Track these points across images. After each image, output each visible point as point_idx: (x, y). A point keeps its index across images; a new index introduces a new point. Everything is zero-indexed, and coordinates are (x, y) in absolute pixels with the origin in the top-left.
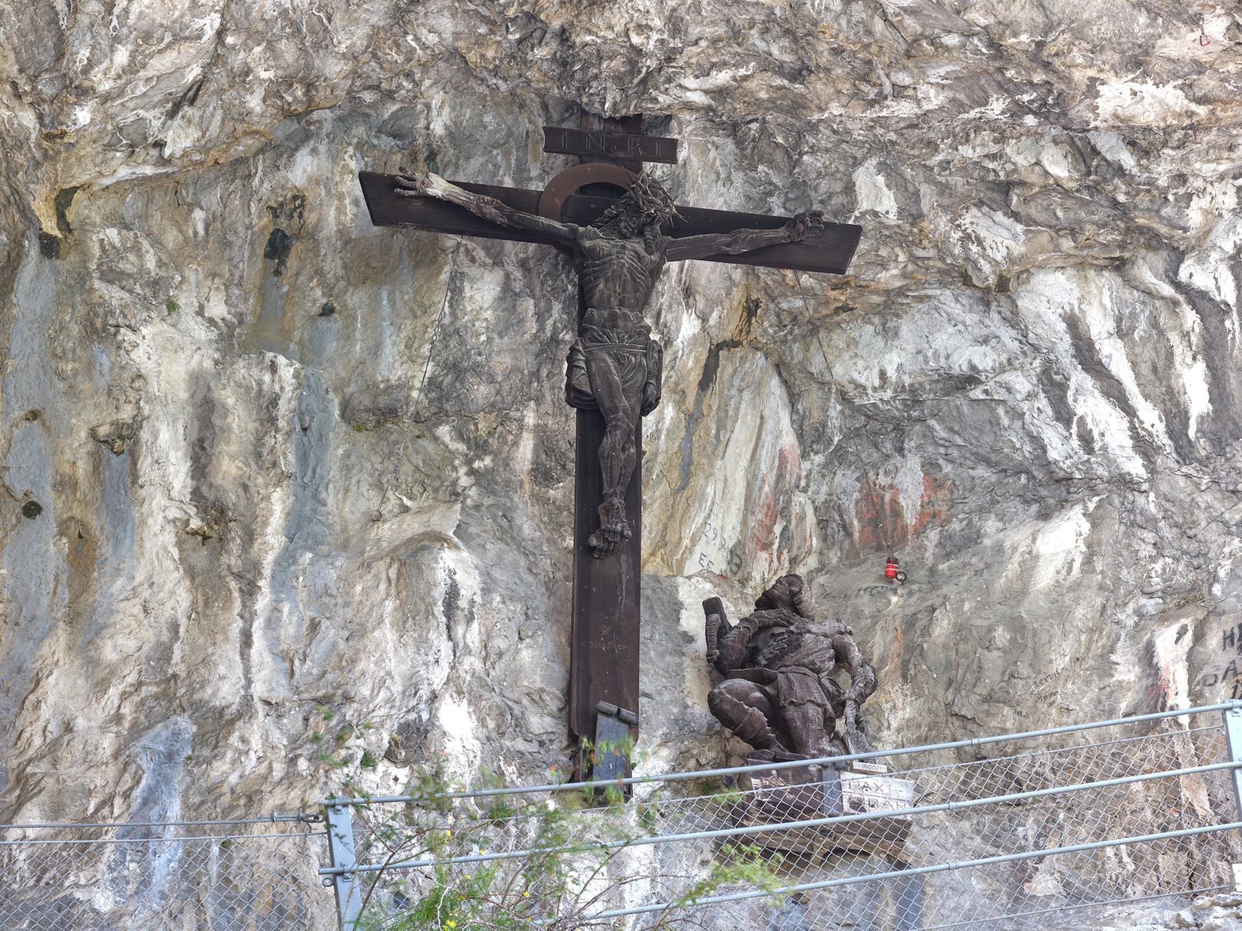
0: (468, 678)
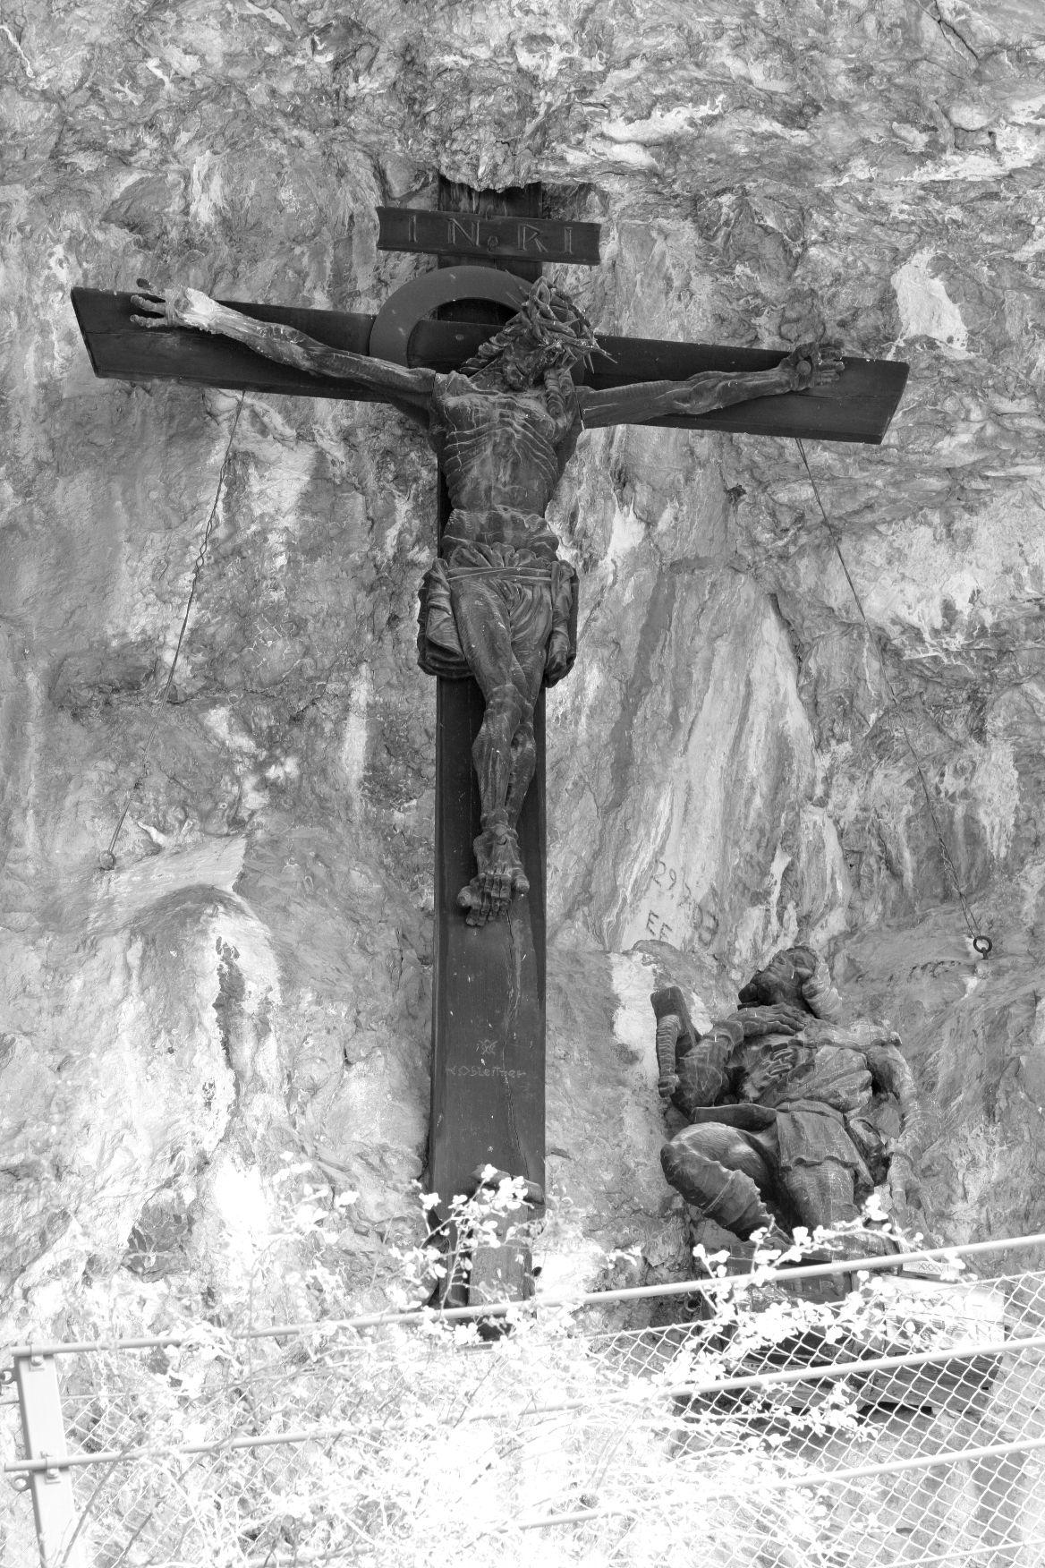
0: (261, 1130)
